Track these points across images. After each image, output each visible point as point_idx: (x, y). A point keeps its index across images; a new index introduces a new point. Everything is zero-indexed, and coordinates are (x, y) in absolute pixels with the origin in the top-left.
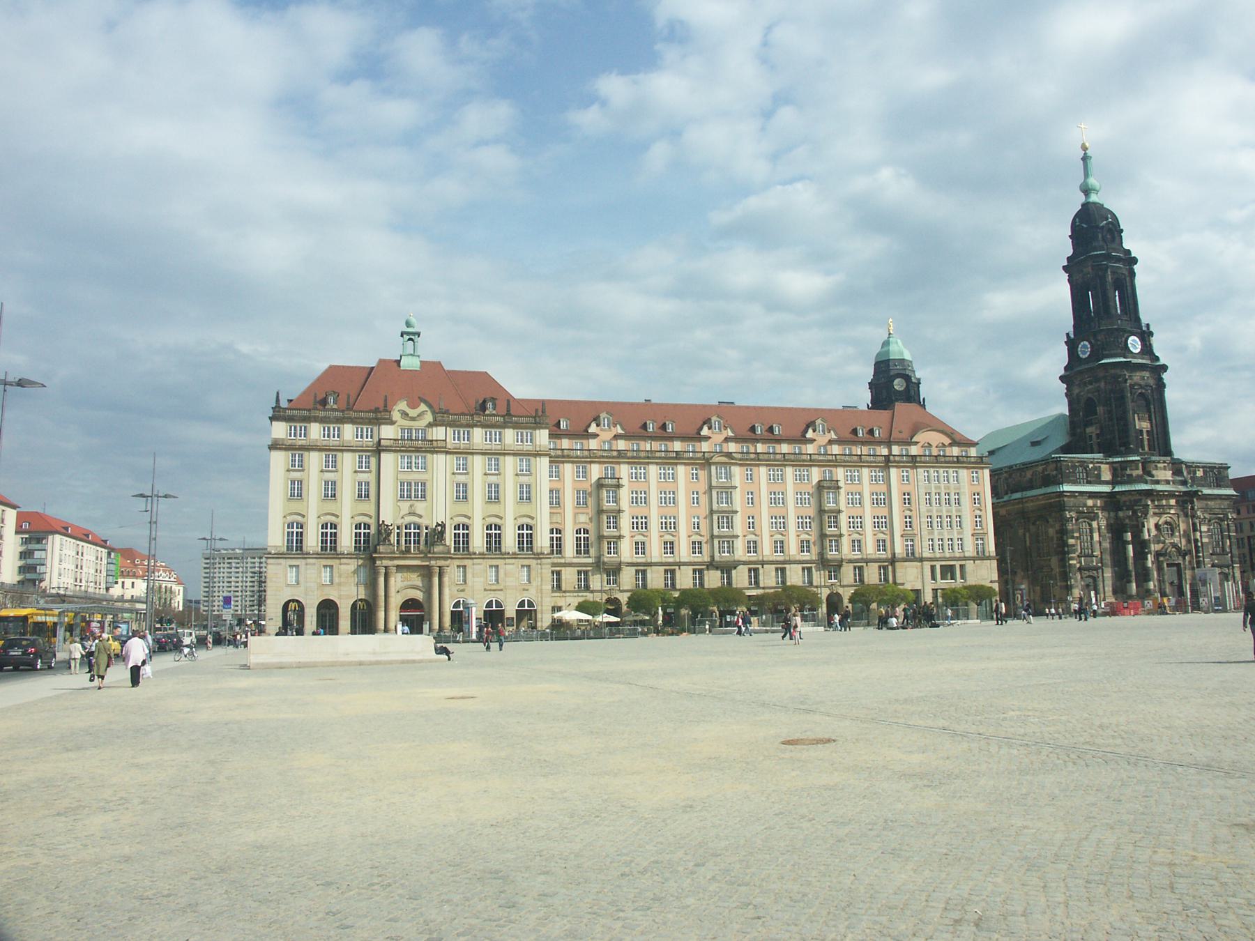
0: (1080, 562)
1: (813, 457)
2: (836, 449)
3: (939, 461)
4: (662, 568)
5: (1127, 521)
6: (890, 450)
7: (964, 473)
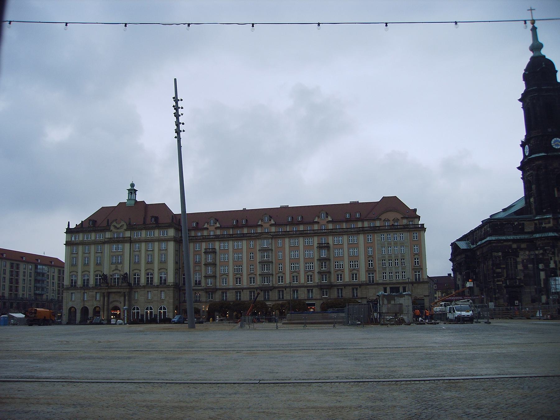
0: (506, 283)
1: (316, 231)
2: (330, 226)
3: (394, 228)
4: (234, 291)
5: (541, 256)
6: (363, 224)
7: (405, 235)
